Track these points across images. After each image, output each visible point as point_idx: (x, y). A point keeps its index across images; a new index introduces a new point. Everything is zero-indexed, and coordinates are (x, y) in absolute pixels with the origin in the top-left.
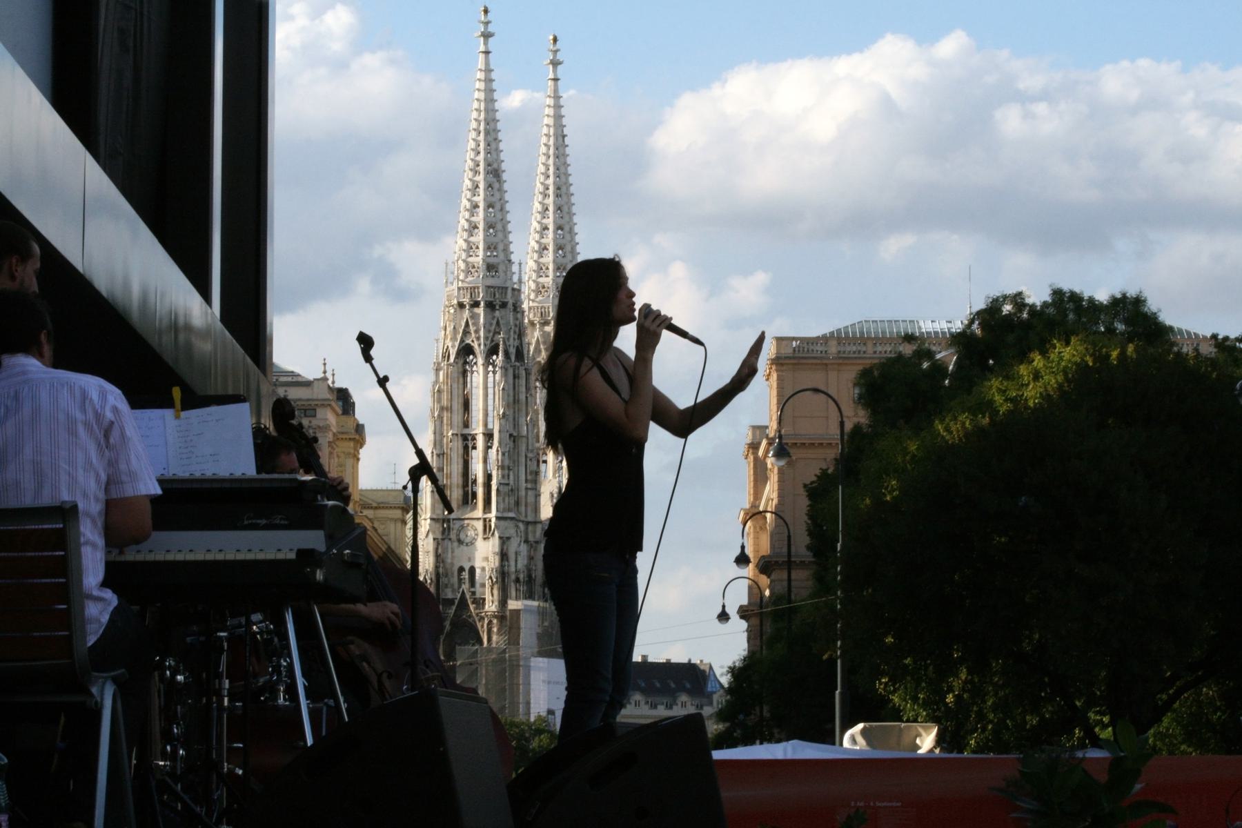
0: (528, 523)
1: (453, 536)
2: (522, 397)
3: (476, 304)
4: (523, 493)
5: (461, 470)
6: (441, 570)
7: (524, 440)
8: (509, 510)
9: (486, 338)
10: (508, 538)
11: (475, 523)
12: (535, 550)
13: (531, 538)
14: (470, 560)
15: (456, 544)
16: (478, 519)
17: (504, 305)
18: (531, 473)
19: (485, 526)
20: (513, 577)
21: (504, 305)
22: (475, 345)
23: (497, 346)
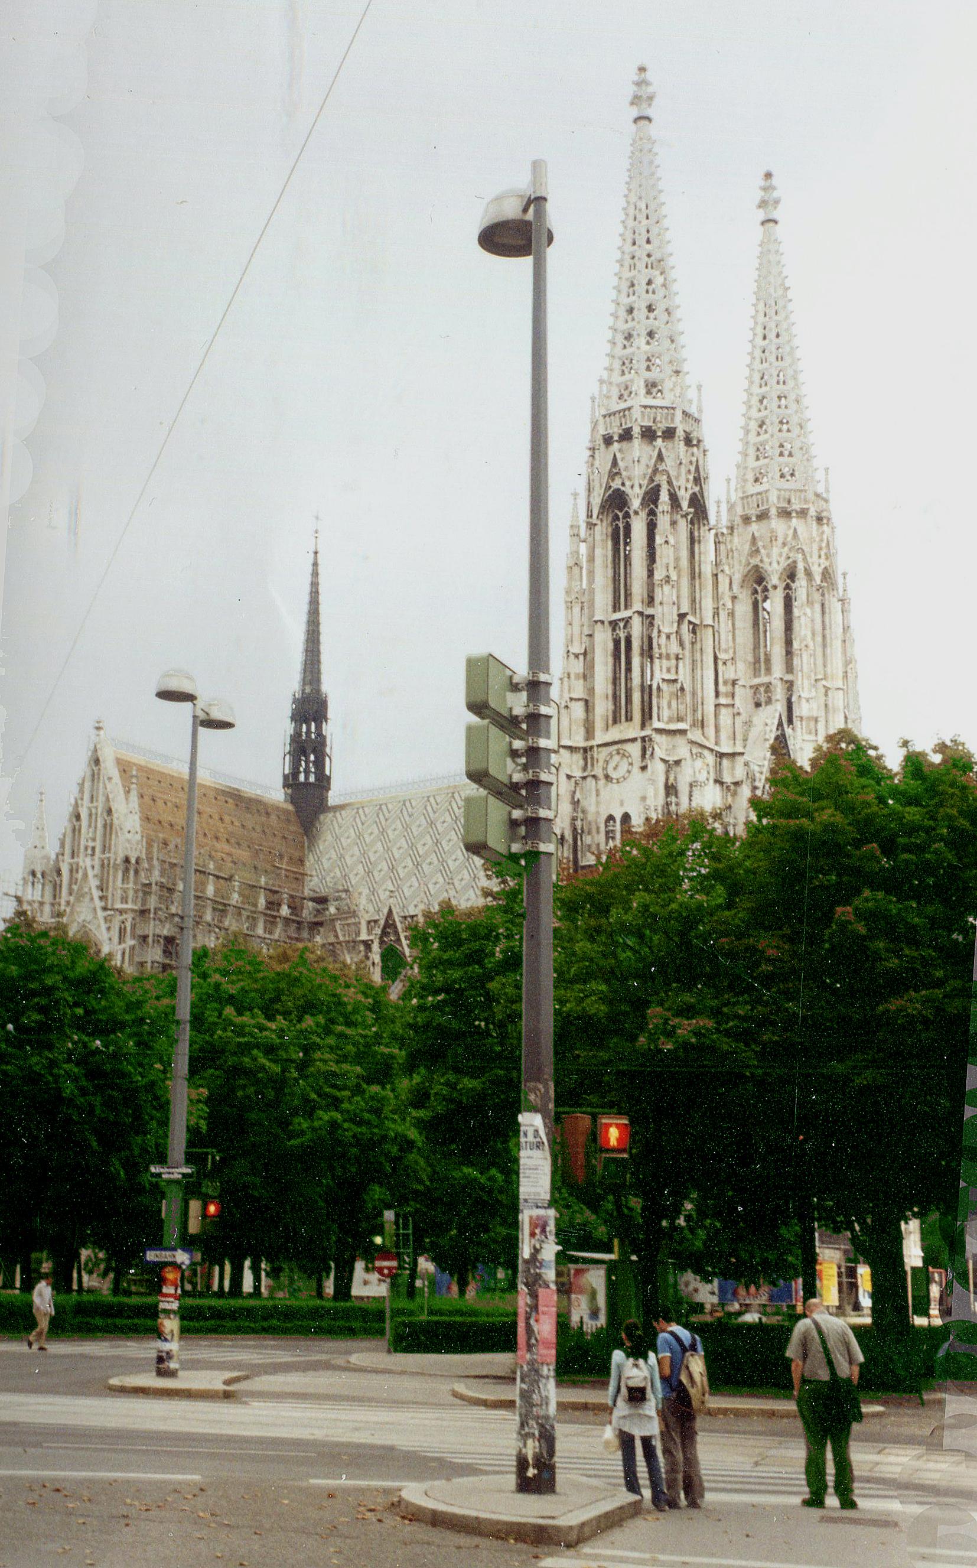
0: (721, 755)
1: (598, 771)
3: (626, 436)
5: (610, 675)
6: (579, 823)
7: (710, 630)
8: (680, 719)
10: (678, 763)
13: (727, 779)
14: (622, 804)
15: (602, 782)
16: (634, 740)
17: (669, 434)
18: (725, 683)
19: (644, 750)
21: (669, 434)
22: (627, 489)
23: (659, 486)
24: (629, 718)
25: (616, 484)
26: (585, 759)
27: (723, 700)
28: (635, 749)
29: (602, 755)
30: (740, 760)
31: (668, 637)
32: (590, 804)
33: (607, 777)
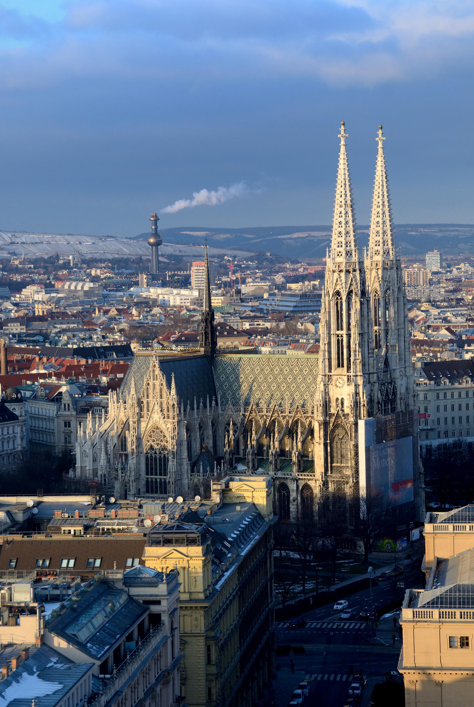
0: (370, 374)
1: (333, 382)
2: (366, 313)
3: (341, 271)
4: (367, 360)
9: (346, 288)
11: (343, 377)
12: (374, 386)
13: (371, 381)
14: (341, 395)
20: (362, 405)
22: (341, 291)
24: (343, 366)
25: (338, 288)
26: (329, 378)
27: (370, 355)
28: (345, 378)
29: (334, 378)
30: (375, 375)
31: (356, 345)
32: (331, 395)
33: (336, 385)
